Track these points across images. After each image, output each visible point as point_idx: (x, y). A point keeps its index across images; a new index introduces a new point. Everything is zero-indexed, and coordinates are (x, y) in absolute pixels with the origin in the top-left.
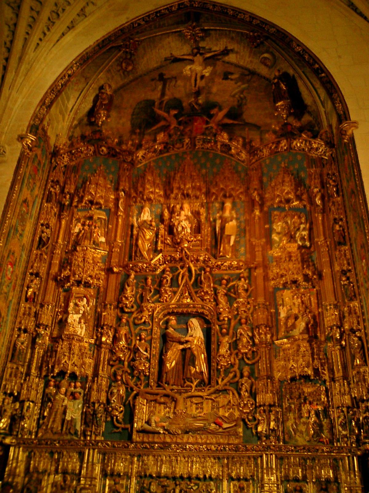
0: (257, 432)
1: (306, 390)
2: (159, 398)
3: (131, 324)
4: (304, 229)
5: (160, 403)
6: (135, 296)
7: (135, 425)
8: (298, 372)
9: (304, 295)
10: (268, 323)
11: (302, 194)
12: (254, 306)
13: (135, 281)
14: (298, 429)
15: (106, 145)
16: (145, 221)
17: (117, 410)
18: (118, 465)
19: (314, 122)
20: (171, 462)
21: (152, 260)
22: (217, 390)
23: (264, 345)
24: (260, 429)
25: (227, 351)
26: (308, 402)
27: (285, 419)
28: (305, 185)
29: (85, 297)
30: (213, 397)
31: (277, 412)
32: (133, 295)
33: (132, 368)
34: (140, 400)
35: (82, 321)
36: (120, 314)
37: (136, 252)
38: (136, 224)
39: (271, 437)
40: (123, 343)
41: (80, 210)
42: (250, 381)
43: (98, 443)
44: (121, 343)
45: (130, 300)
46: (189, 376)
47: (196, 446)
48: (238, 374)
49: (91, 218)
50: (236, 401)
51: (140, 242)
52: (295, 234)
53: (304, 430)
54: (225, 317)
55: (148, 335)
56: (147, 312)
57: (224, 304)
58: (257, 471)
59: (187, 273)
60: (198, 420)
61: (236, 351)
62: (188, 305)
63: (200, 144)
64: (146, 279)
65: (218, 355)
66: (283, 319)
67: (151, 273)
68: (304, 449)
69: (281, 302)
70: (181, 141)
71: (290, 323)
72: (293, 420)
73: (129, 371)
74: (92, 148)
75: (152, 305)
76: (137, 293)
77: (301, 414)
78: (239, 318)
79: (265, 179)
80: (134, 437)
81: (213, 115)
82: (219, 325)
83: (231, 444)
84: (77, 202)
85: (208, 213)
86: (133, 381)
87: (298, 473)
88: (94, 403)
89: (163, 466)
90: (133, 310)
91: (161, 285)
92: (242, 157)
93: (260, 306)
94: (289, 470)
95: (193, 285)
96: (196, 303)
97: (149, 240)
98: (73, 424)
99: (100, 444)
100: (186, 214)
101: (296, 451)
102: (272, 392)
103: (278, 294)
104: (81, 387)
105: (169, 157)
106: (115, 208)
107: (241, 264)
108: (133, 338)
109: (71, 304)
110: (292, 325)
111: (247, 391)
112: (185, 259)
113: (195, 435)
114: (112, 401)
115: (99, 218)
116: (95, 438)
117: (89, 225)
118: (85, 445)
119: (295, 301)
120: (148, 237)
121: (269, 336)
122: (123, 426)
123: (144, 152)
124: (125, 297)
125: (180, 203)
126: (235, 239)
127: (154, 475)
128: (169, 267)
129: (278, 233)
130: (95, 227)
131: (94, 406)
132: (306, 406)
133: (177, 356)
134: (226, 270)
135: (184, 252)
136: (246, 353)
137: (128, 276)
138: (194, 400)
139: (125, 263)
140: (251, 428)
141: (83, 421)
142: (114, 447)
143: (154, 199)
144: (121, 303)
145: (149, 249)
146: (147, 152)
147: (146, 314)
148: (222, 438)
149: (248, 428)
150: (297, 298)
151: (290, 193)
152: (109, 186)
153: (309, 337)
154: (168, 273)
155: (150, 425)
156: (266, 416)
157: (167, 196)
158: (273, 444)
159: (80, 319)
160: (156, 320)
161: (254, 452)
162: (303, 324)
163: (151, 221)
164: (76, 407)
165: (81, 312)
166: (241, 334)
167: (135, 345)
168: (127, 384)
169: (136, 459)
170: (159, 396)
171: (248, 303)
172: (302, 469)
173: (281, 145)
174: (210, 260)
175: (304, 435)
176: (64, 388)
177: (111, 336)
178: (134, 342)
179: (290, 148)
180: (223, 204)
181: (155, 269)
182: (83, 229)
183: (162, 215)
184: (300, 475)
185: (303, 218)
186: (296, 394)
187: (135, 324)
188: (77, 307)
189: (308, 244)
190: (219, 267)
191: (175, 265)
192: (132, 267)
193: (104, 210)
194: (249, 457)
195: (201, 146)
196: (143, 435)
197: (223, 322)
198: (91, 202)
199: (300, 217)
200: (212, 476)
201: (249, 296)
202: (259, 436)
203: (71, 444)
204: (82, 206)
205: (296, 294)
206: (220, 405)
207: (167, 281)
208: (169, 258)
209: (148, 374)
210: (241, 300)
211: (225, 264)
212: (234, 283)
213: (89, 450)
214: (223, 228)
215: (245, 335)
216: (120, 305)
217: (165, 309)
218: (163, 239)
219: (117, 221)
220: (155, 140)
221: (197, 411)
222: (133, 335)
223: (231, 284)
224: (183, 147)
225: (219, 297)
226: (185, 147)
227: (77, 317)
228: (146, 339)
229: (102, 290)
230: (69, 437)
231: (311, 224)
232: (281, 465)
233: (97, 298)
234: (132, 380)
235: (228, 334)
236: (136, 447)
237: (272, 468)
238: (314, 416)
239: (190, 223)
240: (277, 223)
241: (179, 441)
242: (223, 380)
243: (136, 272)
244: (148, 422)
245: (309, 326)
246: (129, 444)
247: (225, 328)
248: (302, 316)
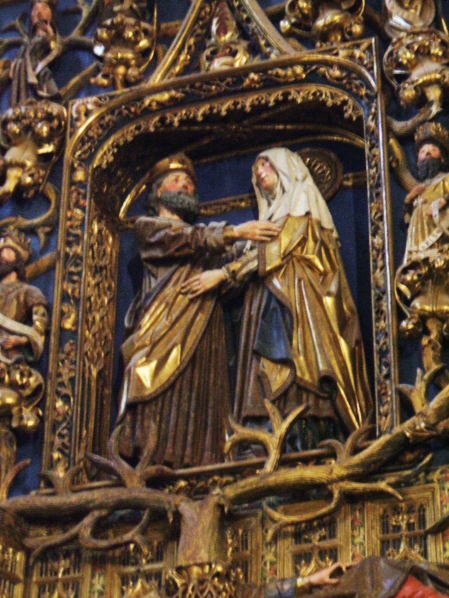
5: (100, 561)
75: (55, 108)
160: (80, 176)
170: (88, 520)
217: (125, 120)
247: (429, 140)
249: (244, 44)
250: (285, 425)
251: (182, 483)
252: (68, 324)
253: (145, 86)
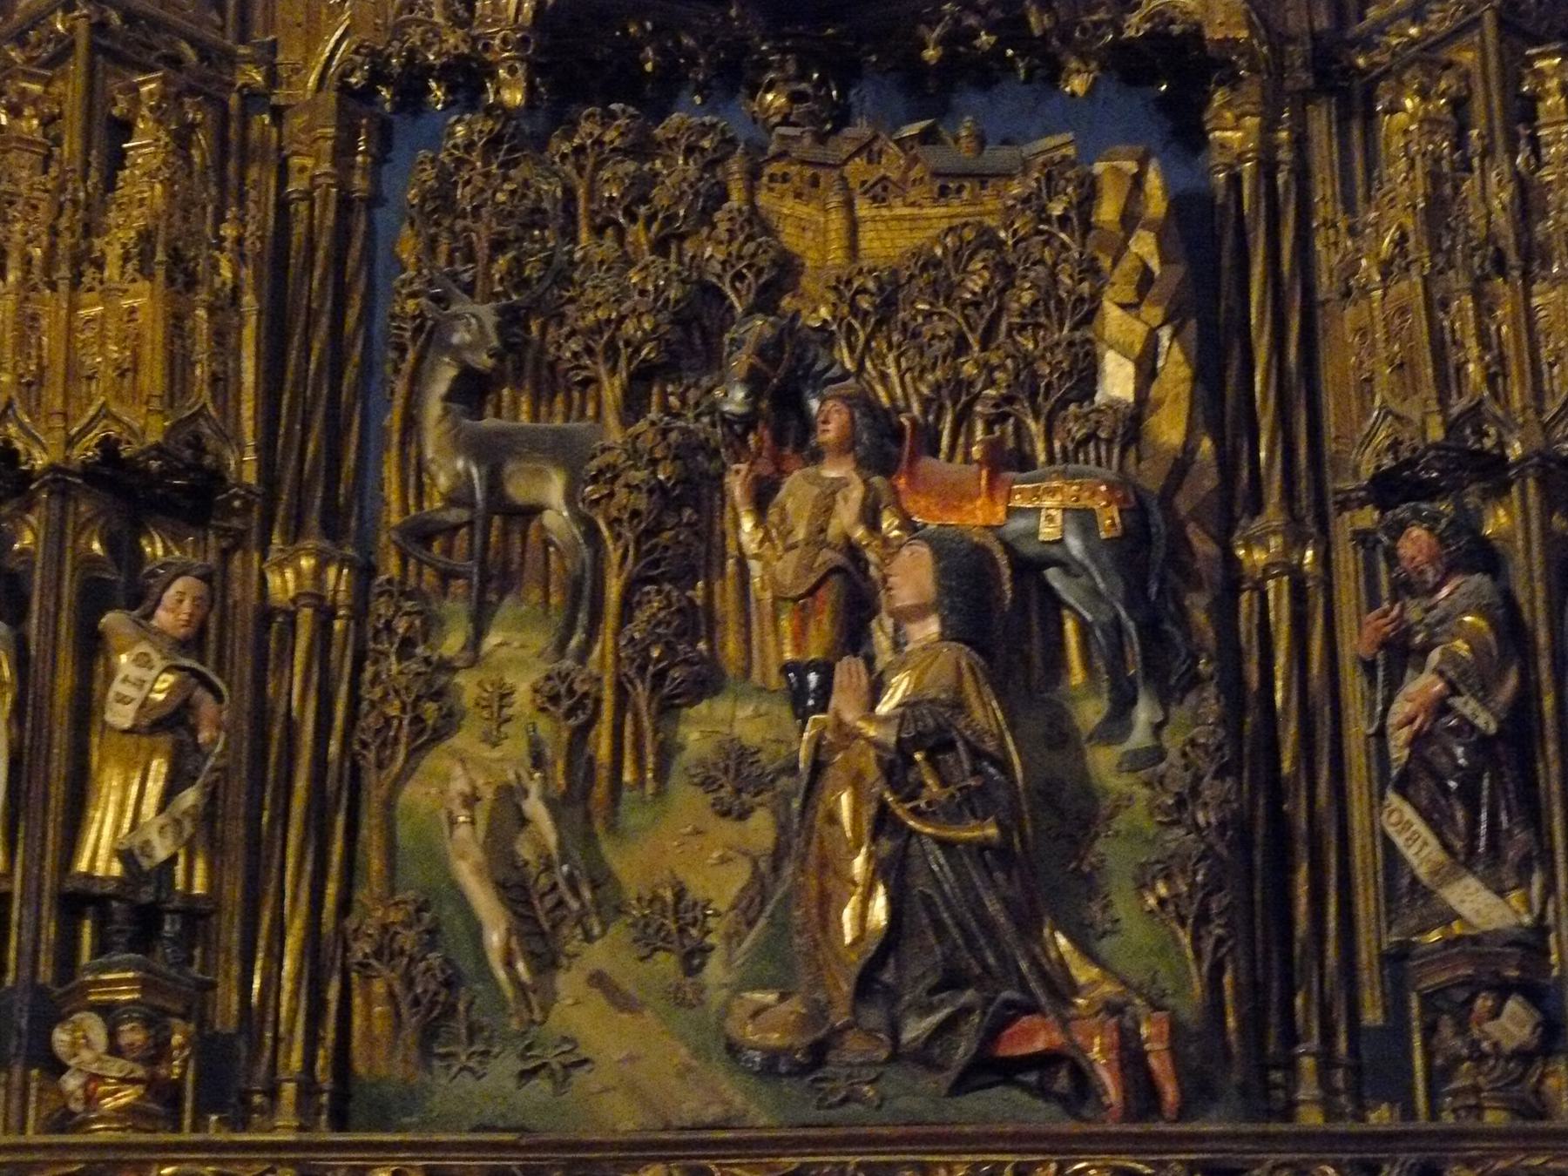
132: (796, 492)
175: (715, 971)
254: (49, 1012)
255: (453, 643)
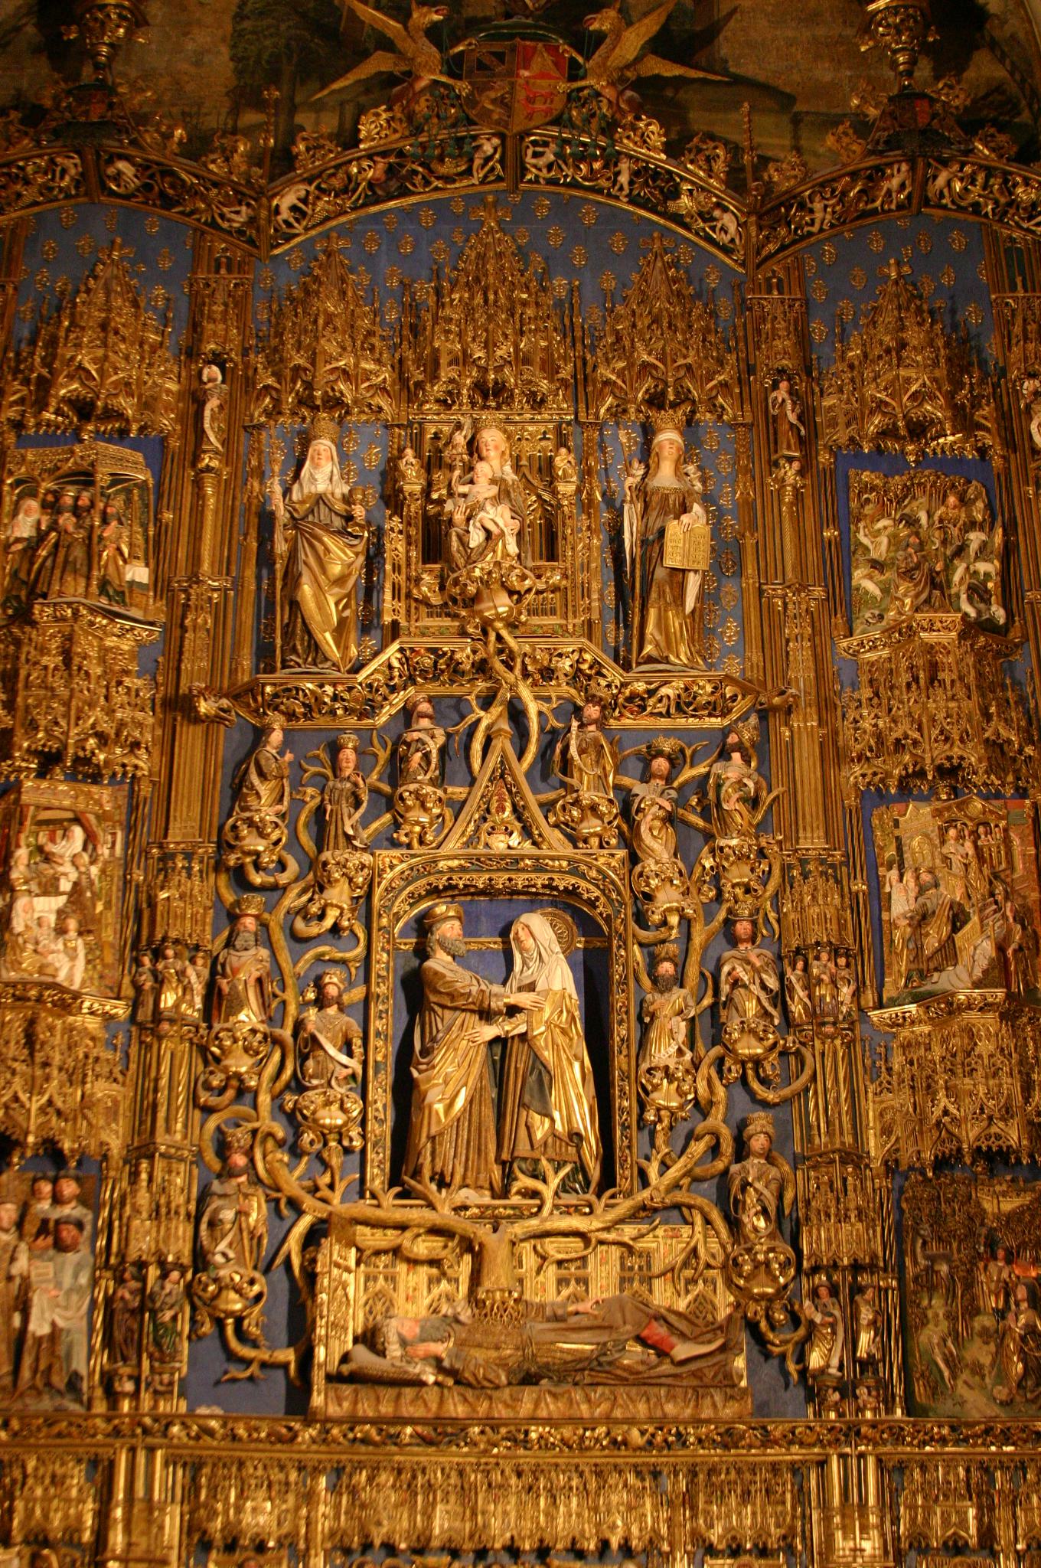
0: (804, 1372)
1: (988, 1206)
2: (406, 1244)
3: (279, 937)
4: (983, 552)
5: (414, 1262)
6: (288, 818)
7: (321, 1353)
8: (970, 1134)
9: (986, 824)
10: (842, 940)
11: (976, 404)
12: (786, 869)
13: (289, 757)
14: (961, 1359)
15: (132, 151)
16: (320, 499)
17: (238, 1291)
18: (254, 1510)
19: (1013, 88)
20: (465, 1492)
21: (356, 669)
22: (644, 1208)
23: (829, 1029)
24: (815, 1360)
25: (680, 1052)
26: (1001, 1253)
27: (913, 1319)
28: (983, 364)
29: (77, 820)
30: (628, 1231)
31: (883, 1292)
32: (283, 816)
33: (294, 1119)
34: (331, 1251)
35: (72, 924)
36: (229, 897)
37: (288, 633)
38: (282, 515)
39: (862, 1392)
40: (249, 1017)
41: (37, 442)
42: (773, 1172)
43: (168, 1425)
44: (242, 1016)
45: (274, 837)
46: (523, 1148)
47: (567, 1432)
48: (727, 1147)
49: (85, 478)
50: (715, 1246)
51: (307, 590)
52: (949, 568)
53: (986, 1360)
54: (670, 910)
55: (351, 984)
56: (344, 885)
57: (665, 857)
58: (806, 1518)
59: (505, 725)
60: (574, 1329)
61: (718, 1050)
62: (513, 862)
63: (541, 162)
64: (335, 749)
65: (644, 1066)
66: (904, 922)
67: (353, 720)
68: (988, 1431)
69: (891, 852)
70: (464, 149)
71: (931, 943)
72: (944, 1325)
73: (280, 1134)
74: (72, 164)
75: (367, 858)
76: (298, 804)
77: (974, 1298)
78: (722, 915)
79: (818, 330)
80: (317, 1400)
81: (600, 38)
82: (641, 945)
83: (708, 1421)
84: (21, 401)
85: (586, 474)
86: (297, 1173)
87: (963, 1523)
88: (141, 1265)
89: (439, 1507)
90: (284, 878)
91: (397, 770)
92: (724, 230)
93: (811, 867)
94: (928, 1512)
95: (528, 775)
96: (545, 851)
97: (340, 581)
98: (61, 1350)
99: (175, 1429)
100: (498, 474)
101: (957, 1443)
102: (860, 1213)
103: (881, 818)
104: (82, 1200)
105: (410, 215)
106: (184, 436)
107: (729, 691)
108: (290, 996)
109: (22, 854)
110: (942, 948)
111: (764, 1212)
112: (499, 666)
113: (565, 1387)
114: (219, 1259)
115: (116, 480)
116: (155, 1406)
117: (76, 511)
118: (117, 1432)
119: (950, 847)
120: (336, 569)
121: (846, 991)
122: (265, 1355)
123: (301, 189)
124: (250, 823)
125: (467, 422)
126: (701, 586)
127: (403, 1546)
128: (430, 700)
129: (877, 565)
130: (105, 521)
131: (144, 1279)
132: (992, 1266)
133: (475, 1071)
134: (668, 715)
135: (492, 637)
136: (757, 1062)
137: (260, 734)
138: (551, 1246)
139: (244, 678)
140: (783, 1357)
141: (98, 1341)
142: (235, 1437)
143: (356, 401)
144: (232, 848)
145: (342, 622)
146: (312, 188)
147: (339, 895)
148: (671, 1397)
149: (767, 1356)
150: (960, 837)
151: (933, 397)
152: (153, 337)
153: (1009, 996)
154: (425, 723)
155: (382, 1353)
156: (843, 1309)
157: (408, 391)
158: (869, 1415)
159: (60, 913)
161: (795, 1449)
162: (987, 949)
163: (348, 500)
164: (67, 1281)
165: (65, 885)
166: (736, 983)
167: (299, 1026)
168: (278, 1190)
169: (323, 1482)
170: (408, 1234)
171: (761, 853)
172: (980, 1508)
173: (885, 185)
174: (599, 674)
176: (9, 1206)
177: (198, 988)
178: (292, 1009)
179: (921, 200)
180: (648, 432)
181: (370, 708)
182: (51, 529)
183: (390, 474)
184: (973, 1530)
185: (980, 505)
186: (956, 1221)
187: (295, 937)
188: (43, 866)
189: (999, 613)
190: (638, 703)
191: (455, 690)
192: (276, 695)
193: (135, 446)
194: (775, 1468)
195: (544, 173)
196: (356, 1392)
197: (662, 933)
198: (84, 409)
199: (964, 501)
200: (634, 1543)
201: (761, 828)
202: (812, 1386)
203: (56, 1429)
204: (38, 425)
205: (951, 822)
206: (657, 1267)
207: (427, 756)
208: (428, 661)
209: (357, 1143)
210: (734, 842)
211: (664, 691)
212: (702, 769)
213: (133, 1450)
214: (654, 542)
215: (755, 989)
216: (232, 860)
218: (402, 579)
219: (199, 494)
220: (352, 140)
221: (565, 1292)
222: (289, 981)
223: (688, 774)
224: (468, 172)
225: (643, 828)
226: (478, 175)
227: (48, 907)
228: (346, 998)
229: (145, 790)
230: (46, 1404)
231: (1010, 529)
232: (895, 1493)
233: (130, 828)
234: (291, 1168)
235: (680, 981)
236: (324, 1438)
237: (863, 1505)
238: (1024, 1305)
239: (516, 513)
240: (875, 520)
241: (501, 1412)
242: (665, 1166)
243: (291, 716)
244: (370, 1338)
245: (1010, 952)
246: (297, 1426)
248: (981, 911)
249: (519, 825)
250: (557, 1181)
251: (476, 1210)
252: (379, 1058)
253: (442, 851)
254: (855, 1388)
255: (925, 1302)
